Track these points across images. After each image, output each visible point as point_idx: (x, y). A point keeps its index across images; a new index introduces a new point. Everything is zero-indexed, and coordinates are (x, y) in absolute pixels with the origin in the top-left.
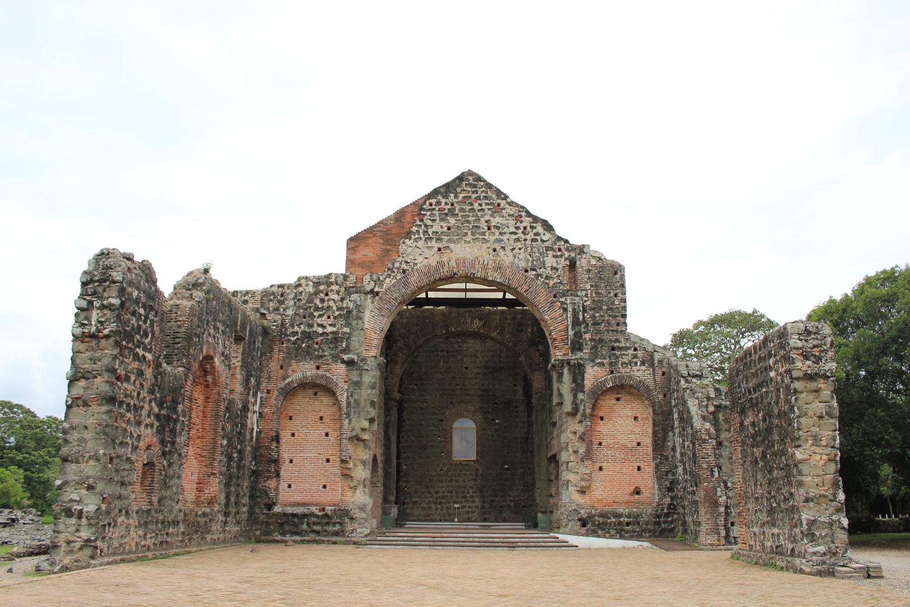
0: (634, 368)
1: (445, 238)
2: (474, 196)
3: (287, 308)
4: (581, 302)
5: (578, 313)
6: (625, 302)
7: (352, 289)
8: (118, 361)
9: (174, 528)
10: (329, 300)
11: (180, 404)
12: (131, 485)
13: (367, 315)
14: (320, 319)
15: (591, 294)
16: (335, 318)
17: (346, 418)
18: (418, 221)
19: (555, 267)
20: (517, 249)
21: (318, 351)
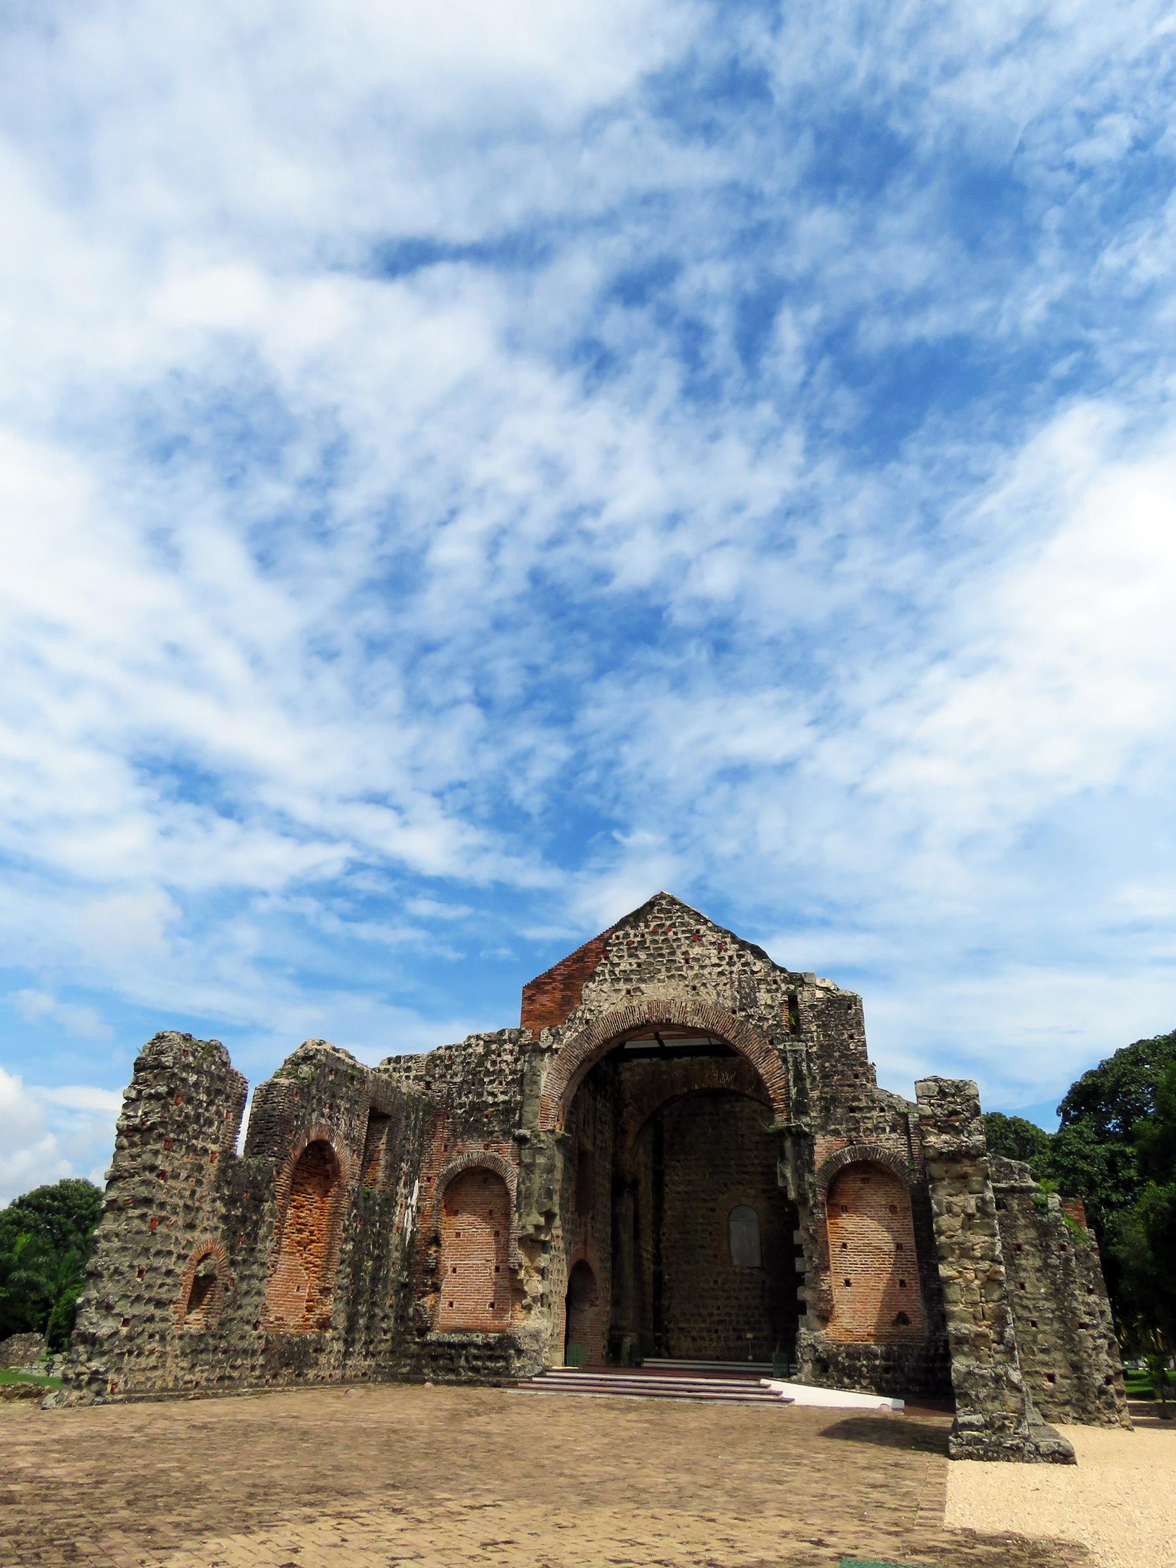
1: (634, 977)
2: (668, 923)
4: (805, 1049)
5: (800, 1063)
6: (864, 1044)
8: (160, 1157)
9: (246, 1359)
10: (500, 1063)
11: (267, 1201)
12: (174, 1303)
13: (544, 1078)
15: (818, 1037)
16: (508, 1083)
20: (721, 984)
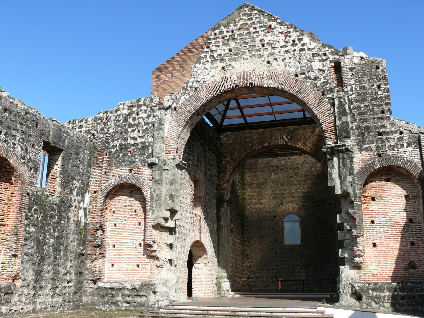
0: (401, 150)
1: (227, 58)
2: (250, 22)
3: (110, 128)
5: (344, 105)
7: (155, 108)
10: (138, 118)
13: (167, 126)
14: (132, 133)
15: (356, 89)
16: (143, 131)
17: (150, 209)
18: (206, 48)
19: (321, 70)
21: (131, 157)
